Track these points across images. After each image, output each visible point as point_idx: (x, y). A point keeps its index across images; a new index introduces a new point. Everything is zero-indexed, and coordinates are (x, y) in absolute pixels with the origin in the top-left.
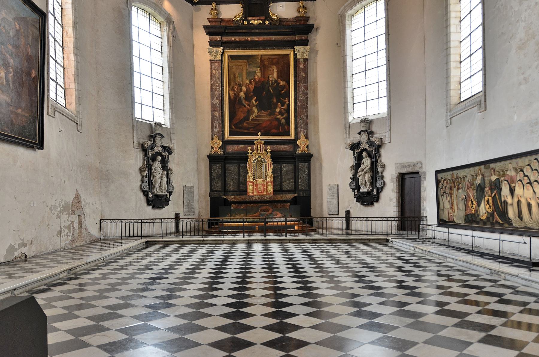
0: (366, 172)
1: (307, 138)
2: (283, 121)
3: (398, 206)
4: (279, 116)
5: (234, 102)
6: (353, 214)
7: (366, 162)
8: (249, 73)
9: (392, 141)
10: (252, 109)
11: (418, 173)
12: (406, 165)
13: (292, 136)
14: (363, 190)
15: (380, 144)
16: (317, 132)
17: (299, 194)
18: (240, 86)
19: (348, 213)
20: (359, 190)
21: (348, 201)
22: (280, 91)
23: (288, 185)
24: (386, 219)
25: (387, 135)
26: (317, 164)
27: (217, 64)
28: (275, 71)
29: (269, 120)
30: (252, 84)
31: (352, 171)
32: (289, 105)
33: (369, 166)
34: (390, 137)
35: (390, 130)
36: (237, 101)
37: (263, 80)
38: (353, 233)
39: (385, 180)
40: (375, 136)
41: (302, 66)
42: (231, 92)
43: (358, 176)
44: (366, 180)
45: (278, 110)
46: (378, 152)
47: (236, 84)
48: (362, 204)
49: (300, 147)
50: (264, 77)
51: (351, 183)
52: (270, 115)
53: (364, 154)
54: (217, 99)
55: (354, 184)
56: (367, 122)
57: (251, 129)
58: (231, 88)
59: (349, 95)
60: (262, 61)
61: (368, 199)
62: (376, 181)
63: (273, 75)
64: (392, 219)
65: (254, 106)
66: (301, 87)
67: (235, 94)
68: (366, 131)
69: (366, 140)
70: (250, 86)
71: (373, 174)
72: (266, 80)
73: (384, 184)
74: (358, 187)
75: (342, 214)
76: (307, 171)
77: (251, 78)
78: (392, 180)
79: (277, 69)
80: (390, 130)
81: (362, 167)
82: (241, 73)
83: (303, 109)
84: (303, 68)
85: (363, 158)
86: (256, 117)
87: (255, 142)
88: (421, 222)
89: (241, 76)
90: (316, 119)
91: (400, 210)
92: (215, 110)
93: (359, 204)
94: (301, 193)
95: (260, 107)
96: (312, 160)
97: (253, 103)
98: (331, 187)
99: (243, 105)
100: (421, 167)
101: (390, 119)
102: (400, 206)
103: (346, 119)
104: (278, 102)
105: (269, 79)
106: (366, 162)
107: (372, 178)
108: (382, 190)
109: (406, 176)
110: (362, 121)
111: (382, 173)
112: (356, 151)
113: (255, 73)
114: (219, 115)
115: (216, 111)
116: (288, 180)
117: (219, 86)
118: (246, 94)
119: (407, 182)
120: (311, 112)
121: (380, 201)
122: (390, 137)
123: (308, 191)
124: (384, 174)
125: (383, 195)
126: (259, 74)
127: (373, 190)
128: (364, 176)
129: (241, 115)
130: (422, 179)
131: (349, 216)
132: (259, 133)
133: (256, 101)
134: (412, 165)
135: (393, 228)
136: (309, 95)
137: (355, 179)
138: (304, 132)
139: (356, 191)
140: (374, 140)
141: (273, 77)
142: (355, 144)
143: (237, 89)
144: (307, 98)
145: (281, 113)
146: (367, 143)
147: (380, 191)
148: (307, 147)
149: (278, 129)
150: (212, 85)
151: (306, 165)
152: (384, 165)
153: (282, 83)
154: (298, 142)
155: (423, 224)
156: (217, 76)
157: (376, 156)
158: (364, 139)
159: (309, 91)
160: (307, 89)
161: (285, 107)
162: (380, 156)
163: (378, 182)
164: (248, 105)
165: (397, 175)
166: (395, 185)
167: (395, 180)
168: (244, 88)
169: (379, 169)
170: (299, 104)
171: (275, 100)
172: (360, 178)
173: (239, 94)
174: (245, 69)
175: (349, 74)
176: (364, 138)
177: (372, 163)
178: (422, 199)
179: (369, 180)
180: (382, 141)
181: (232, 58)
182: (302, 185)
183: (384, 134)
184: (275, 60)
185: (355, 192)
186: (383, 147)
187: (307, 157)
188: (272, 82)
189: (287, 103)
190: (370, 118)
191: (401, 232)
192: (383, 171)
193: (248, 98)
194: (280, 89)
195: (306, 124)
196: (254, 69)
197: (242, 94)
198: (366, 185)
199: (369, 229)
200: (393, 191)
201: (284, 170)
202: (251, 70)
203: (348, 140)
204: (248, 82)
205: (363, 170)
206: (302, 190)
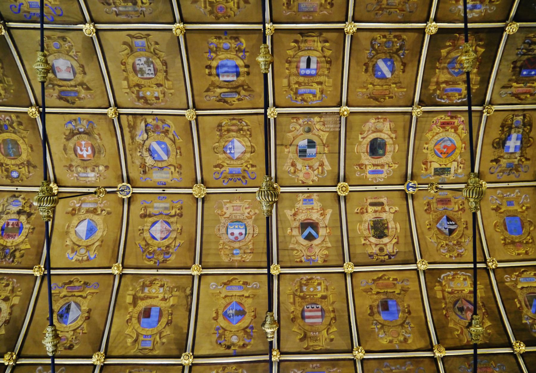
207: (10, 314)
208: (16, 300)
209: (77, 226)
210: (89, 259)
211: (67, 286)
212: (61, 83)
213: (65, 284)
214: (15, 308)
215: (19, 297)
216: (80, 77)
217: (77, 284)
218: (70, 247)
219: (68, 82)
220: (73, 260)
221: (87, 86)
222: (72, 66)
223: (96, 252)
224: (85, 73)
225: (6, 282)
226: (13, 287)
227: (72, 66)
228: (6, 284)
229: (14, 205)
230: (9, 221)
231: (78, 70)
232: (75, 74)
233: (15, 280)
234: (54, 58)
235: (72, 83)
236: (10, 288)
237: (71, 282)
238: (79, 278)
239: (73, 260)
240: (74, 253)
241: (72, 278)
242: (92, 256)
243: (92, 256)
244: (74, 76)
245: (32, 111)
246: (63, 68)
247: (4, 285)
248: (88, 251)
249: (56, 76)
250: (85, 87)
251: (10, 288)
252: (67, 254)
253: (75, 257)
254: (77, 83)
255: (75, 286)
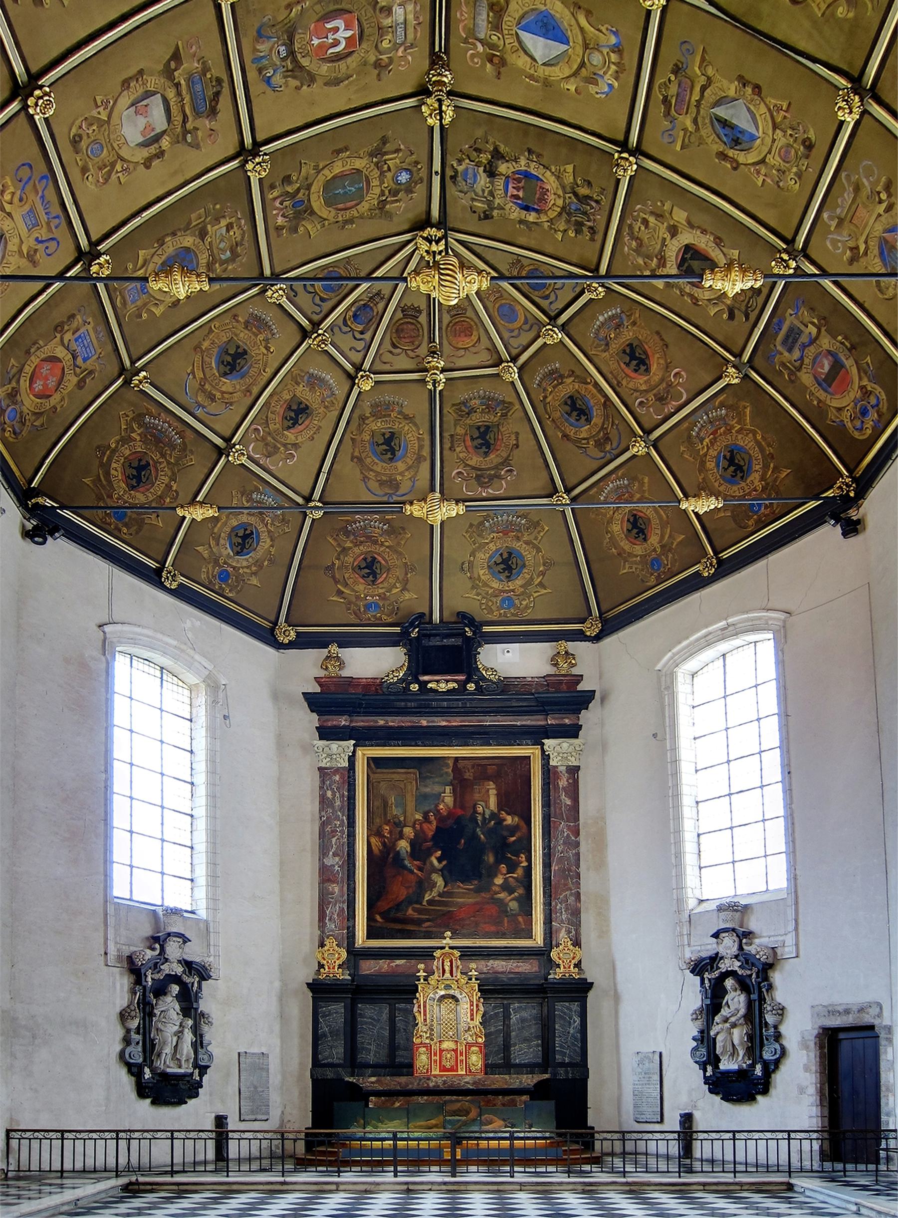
0: (734, 1025)
1: (577, 943)
2: (514, 905)
3: (821, 1105)
4: (502, 896)
5: (382, 864)
6: (701, 1122)
7: (735, 1001)
8: (422, 798)
9: (801, 953)
10: (430, 879)
11: (871, 1028)
12: (840, 1009)
13: (538, 939)
14: (726, 1065)
15: (770, 961)
16: (604, 932)
17: (554, 1074)
18: (398, 825)
19: (687, 1119)
20: (716, 1066)
21: (686, 1088)
22: (505, 838)
23: (525, 1051)
24: (785, 1135)
25: (790, 940)
26: (606, 1005)
27: (337, 778)
28: (493, 792)
29: (476, 903)
30: (430, 823)
31: (699, 1023)
32: (528, 870)
33: (742, 1011)
34: (797, 945)
35: (796, 929)
36: (390, 860)
37: (459, 812)
38: (697, 1166)
39: (784, 1043)
40: (757, 941)
41: (563, 783)
42: (373, 840)
43: (712, 1033)
44: (736, 1042)
45: (499, 881)
46: (766, 979)
47: (388, 823)
48: (725, 1098)
49: (558, 966)
50: (462, 807)
51: (695, 1049)
52: (478, 890)
53: (729, 983)
54: (335, 855)
55: (704, 1051)
56: (738, 909)
57: (428, 924)
58: (374, 831)
59: (689, 847)
60: (456, 769)
61: (741, 1086)
62: (762, 1045)
63: (487, 802)
64: (803, 1135)
65: (434, 870)
66: (563, 828)
67: (384, 844)
68: (734, 930)
69: (735, 950)
70: (425, 826)
71: (754, 1028)
72: (469, 814)
73: (784, 1052)
74: (713, 1059)
75: (673, 1123)
76: (578, 1020)
77: (427, 809)
78: (804, 1045)
79: (498, 789)
80: (796, 929)
81: (725, 1012)
82: (402, 796)
83: (564, 881)
84: (565, 788)
85: (725, 992)
86: (440, 895)
87: (437, 953)
88: (883, 1146)
89: (403, 805)
90: (603, 902)
91: (826, 1113)
92: (329, 880)
93: (717, 1099)
94: (561, 1071)
95: (452, 873)
96: (591, 995)
97: (431, 863)
98: (642, 1058)
99: (405, 867)
100: (880, 1015)
101: (796, 903)
102: (826, 1104)
103: (680, 901)
104: (498, 862)
105: (475, 812)
106: (735, 1001)
107: (751, 1037)
108: (777, 1067)
109: (842, 1036)
110: (720, 909)
111: (776, 1027)
112: (706, 975)
113: (438, 797)
114: (341, 890)
115: (334, 882)
116: (526, 1040)
117: (342, 825)
118: (413, 843)
119: (845, 1048)
120: (589, 882)
121: (772, 1091)
122: (797, 945)
123: (581, 1066)
124: (783, 1029)
125: (780, 1079)
126: (449, 800)
127: (753, 1066)
128: (730, 1034)
129: (399, 891)
130: (883, 1042)
131: (690, 1127)
132: (449, 933)
133: (439, 860)
134: (855, 1008)
135: (806, 1156)
136: (583, 848)
137: (705, 1040)
138: (569, 932)
139: (709, 1068)
140: (753, 952)
141: (487, 806)
142: (704, 959)
143: (390, 832)
144: (578, 854)
145: (507, 887)
146: (736, 957)
147: (771, 1068)
148: (578, 965)
149: (500, 923)
150: (323, 825)
151: (575, 1006)
152: (783, 1009)
153: (509, 820)
154: (554, 954)
155: (887, 1150)
156: (338, 803)
157: (760, 989)
158: (729, 948)
159: (582, 838)
160: (577, 833)
161: (520, 872)
162: (770, 987)
163: (765, 1048)
164: (420, 869)
165: (816, 1032)
166: (812, 1055)
167: (812, 1045)
168: (408, 831)
169: (770, 1019)
170: (554, 867)
171: (491, 859)
172: (719, 1038)
173: (394, 845)
174: (412, 787)
175: (687, 801)
176: (728, 946)
177: (750, 1004)
178: (883, 1088)
179: (741, 1043)
180: (775, 954)
181: (376, 763)
182: (564, 1052)
183: (781, 938)
184: (491, 770)
185: (705, 1071)
186: (778, 967)
187: (579, 990)
188: (484, 818)
189: (525, 864)
190: (743, 902)
191: (828, 1165)
192: (781, 1022)
193: (419, 851)
194: (505, 833)
195: (576, 913)
196: (437, 789)
197: (403, 845)
198: (734, 1053)
199: (740, 1157)
200: (806, 1069)
201: (514, 1018)
202: (428, 790)
203: (687, 949)
204: (419, 816)
205: (726, 1020)
206: (562, 1065)
207: (704, 232)
208: (680, 216)
209: (533, 59)
210: (617, 49)
211: (673, 112)
212: (178, 118)
213: (667, 113)
214: (695, 221)
215: (675, 208)
216: (153, 82)
217: (673, 89)
218: (582, 84)
219: (172, 104)
220: (616, 84)
221: (169, 61)
222: (132, 105)
223: (603, 29)
224: (141, 72)
225: (639, 224)
226: (652, 213)
227: (132, 105)
228: (642, 223)
229: (475, 182)
230: (509, 194)
231: (137, 90)
232: (148, 94)
233: (639, 206)
234: (124, 148)
235: (171, 94)
236: (652, 220)
237: (666, 101)
238: (658, 81)
239: (616, 84)
240: (600, 80)
241: (658, 96)
242: (613, 40)
243: (613, 40)
244: (154, 93)
245: (256, 171)
246: (141, 122)
247: (643, 228)
248: (597, 47)
249: (164, 132)
250: (173, 65)
251: (652, 220)
252: (598, 96)
253: (609, 79)
254: (168, 83)
255: (678, 95)
